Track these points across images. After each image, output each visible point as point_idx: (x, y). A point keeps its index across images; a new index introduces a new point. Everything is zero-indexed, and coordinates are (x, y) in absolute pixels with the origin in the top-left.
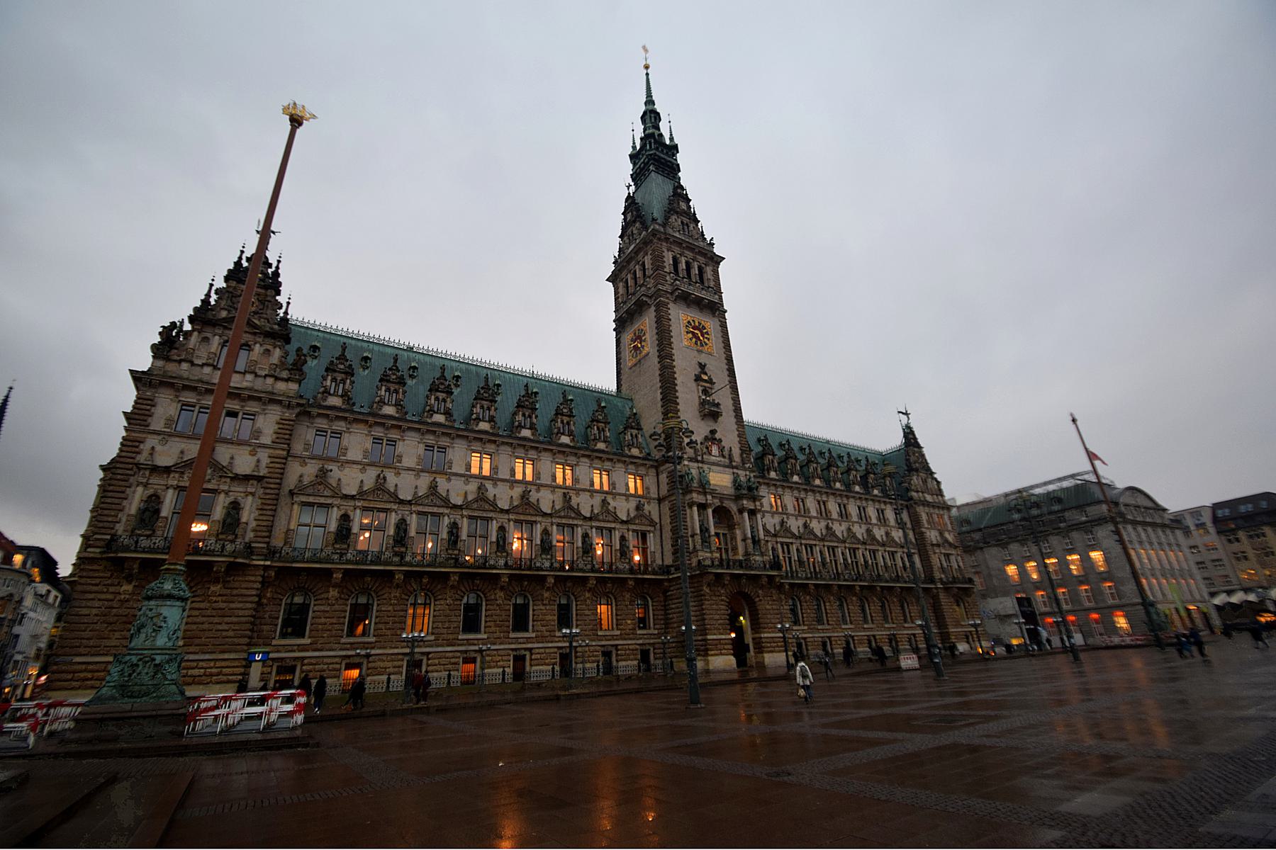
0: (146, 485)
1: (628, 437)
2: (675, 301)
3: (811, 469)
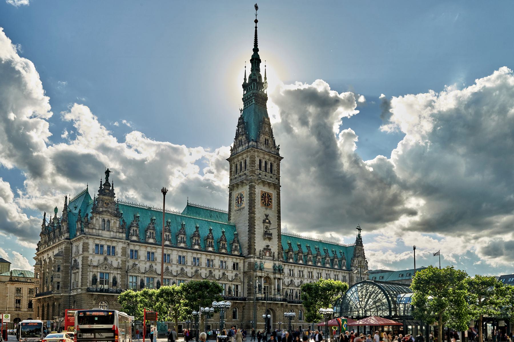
0: (92, 272)
1: (234, 247)
2: (258, 184)
3: (308, 258)
